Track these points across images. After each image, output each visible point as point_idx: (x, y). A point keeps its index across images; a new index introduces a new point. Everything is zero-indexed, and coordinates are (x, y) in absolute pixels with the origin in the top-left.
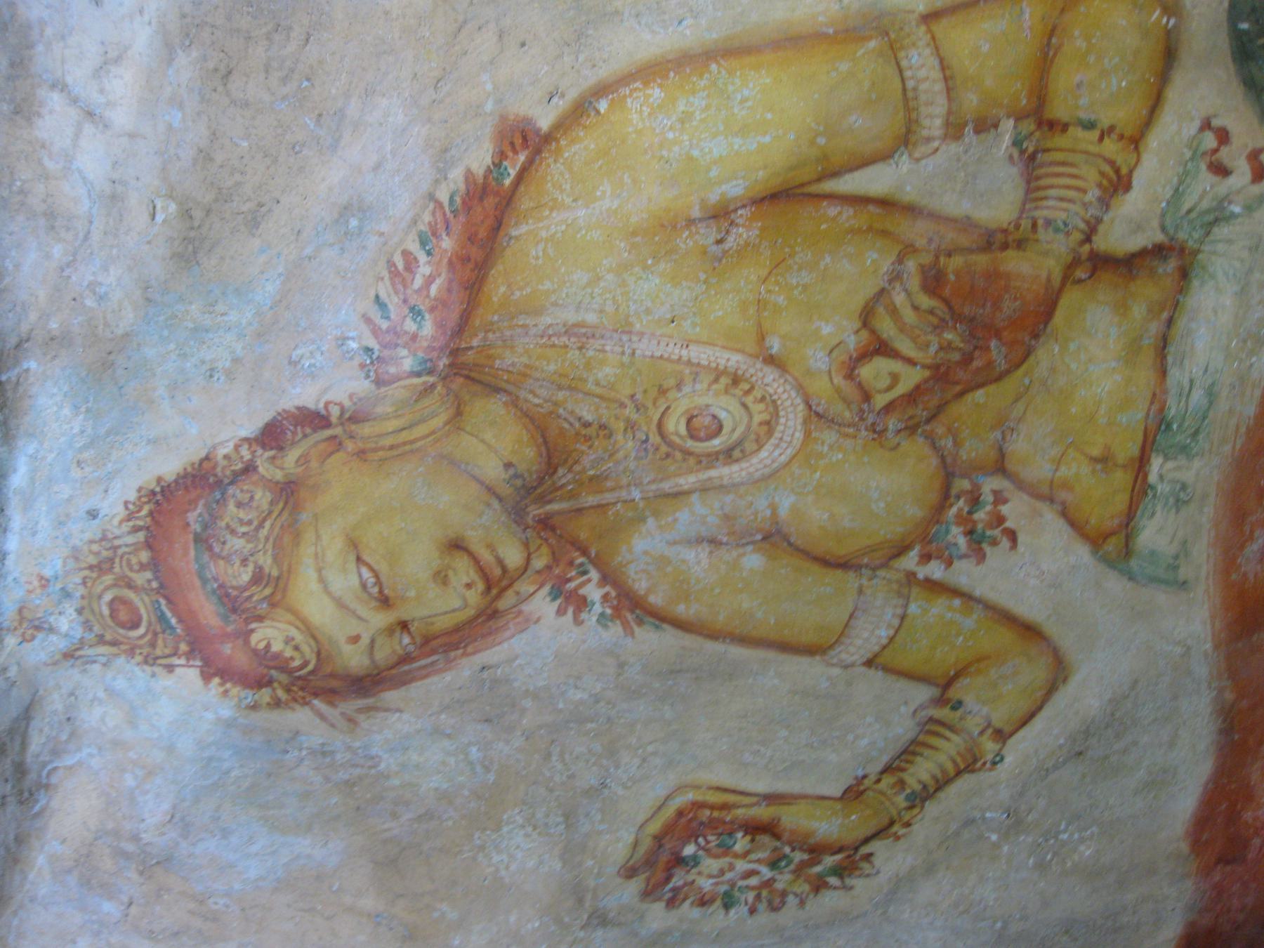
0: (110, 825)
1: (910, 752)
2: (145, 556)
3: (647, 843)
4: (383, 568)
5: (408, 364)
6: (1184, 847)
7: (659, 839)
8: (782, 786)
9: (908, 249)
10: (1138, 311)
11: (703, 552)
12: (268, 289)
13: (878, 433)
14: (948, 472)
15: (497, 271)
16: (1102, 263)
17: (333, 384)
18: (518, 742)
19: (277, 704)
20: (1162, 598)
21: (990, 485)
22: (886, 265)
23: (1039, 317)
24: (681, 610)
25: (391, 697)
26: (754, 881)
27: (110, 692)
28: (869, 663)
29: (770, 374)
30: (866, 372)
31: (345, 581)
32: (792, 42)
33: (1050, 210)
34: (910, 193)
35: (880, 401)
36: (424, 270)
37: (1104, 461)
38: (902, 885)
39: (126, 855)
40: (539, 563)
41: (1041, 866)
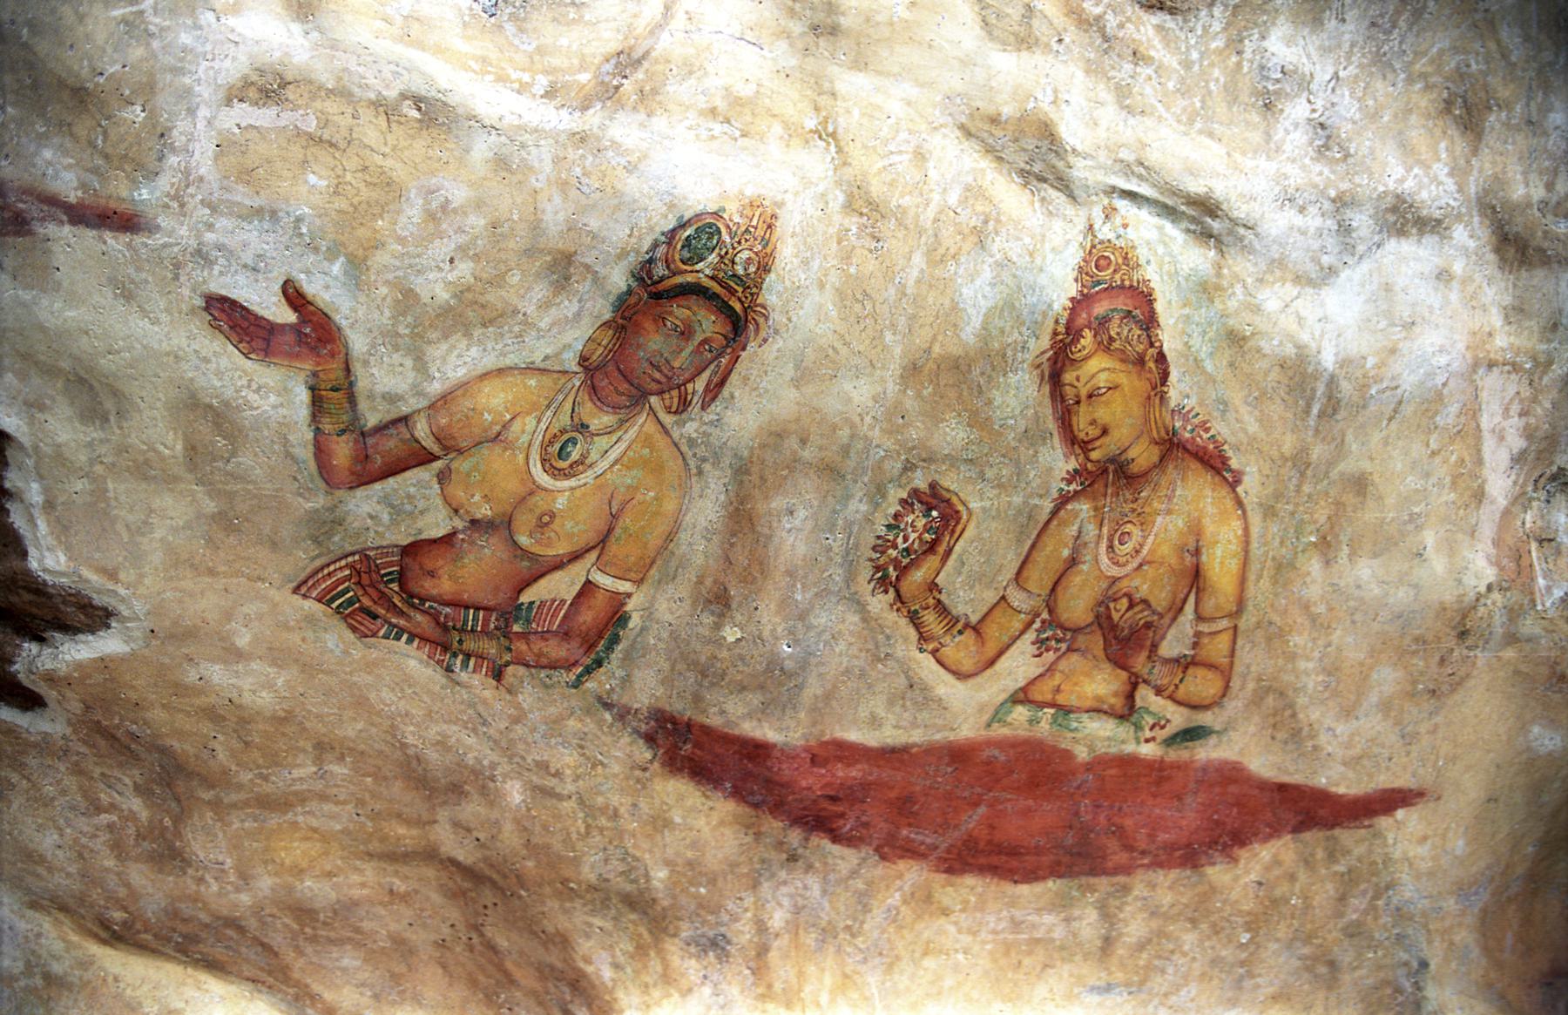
0: (1003, 218)
1: (942, 609)
2: (1127, 283)
3: (948, 496)
4: (1104, 398)
5: (1178, 425)
6: (827, 738)
7: (948, 501)
8: (954, 556)
9: (1161, 616)
10: (1113, 700)
11: (1075, 533)
12: (1209, 366)
13: (1100, 604)
14: (1077, 630)
15: (1199, 465)
16: (1134, 686)
17: (1179, 389)
18: (1013, 444)
19: (1055, 333)
20: (986, 717)
21: (1064, 646)
22: (1159, 609)
23: (1119, 663)
24: (1055, 522)
25: (1047, 389)
26: (900, 540)
27: (1068, 242)
28: (1003, 598)
29: (1135, 565)
30: (1125, 601)
31: (1102, 380)
32: (1243, 581)
33: (1158, 666)
34: (1181, 619)
35: (1112, 605)
36: (1205, 436)
37: (1058, 690)
38: (861, 607)
39: (986, 222)
40: (1089, 465)
41: (847, 671)
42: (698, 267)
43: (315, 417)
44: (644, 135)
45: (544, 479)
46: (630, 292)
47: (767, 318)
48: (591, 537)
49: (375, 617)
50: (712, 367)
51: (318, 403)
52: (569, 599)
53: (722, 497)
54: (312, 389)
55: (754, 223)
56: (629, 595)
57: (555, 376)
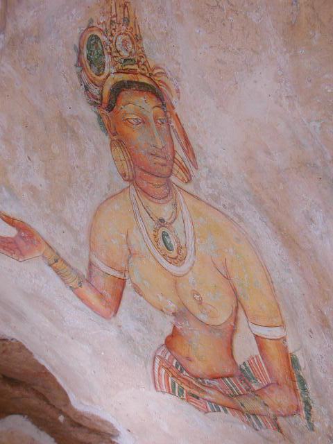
42: (107, 71)
43: (63, 280)
44: (31, 13)
45: (173, 268)
46: (100, 117)
47: (164, 74)
48: (229, 302)
49: (198, 398)
50: (173, 134)
51: (57, 271)
52: (257, 352)
53: (269, 231)
54: (50, 265)
55: (114, 13)
56: (284, 339)
57: (122, 195)
